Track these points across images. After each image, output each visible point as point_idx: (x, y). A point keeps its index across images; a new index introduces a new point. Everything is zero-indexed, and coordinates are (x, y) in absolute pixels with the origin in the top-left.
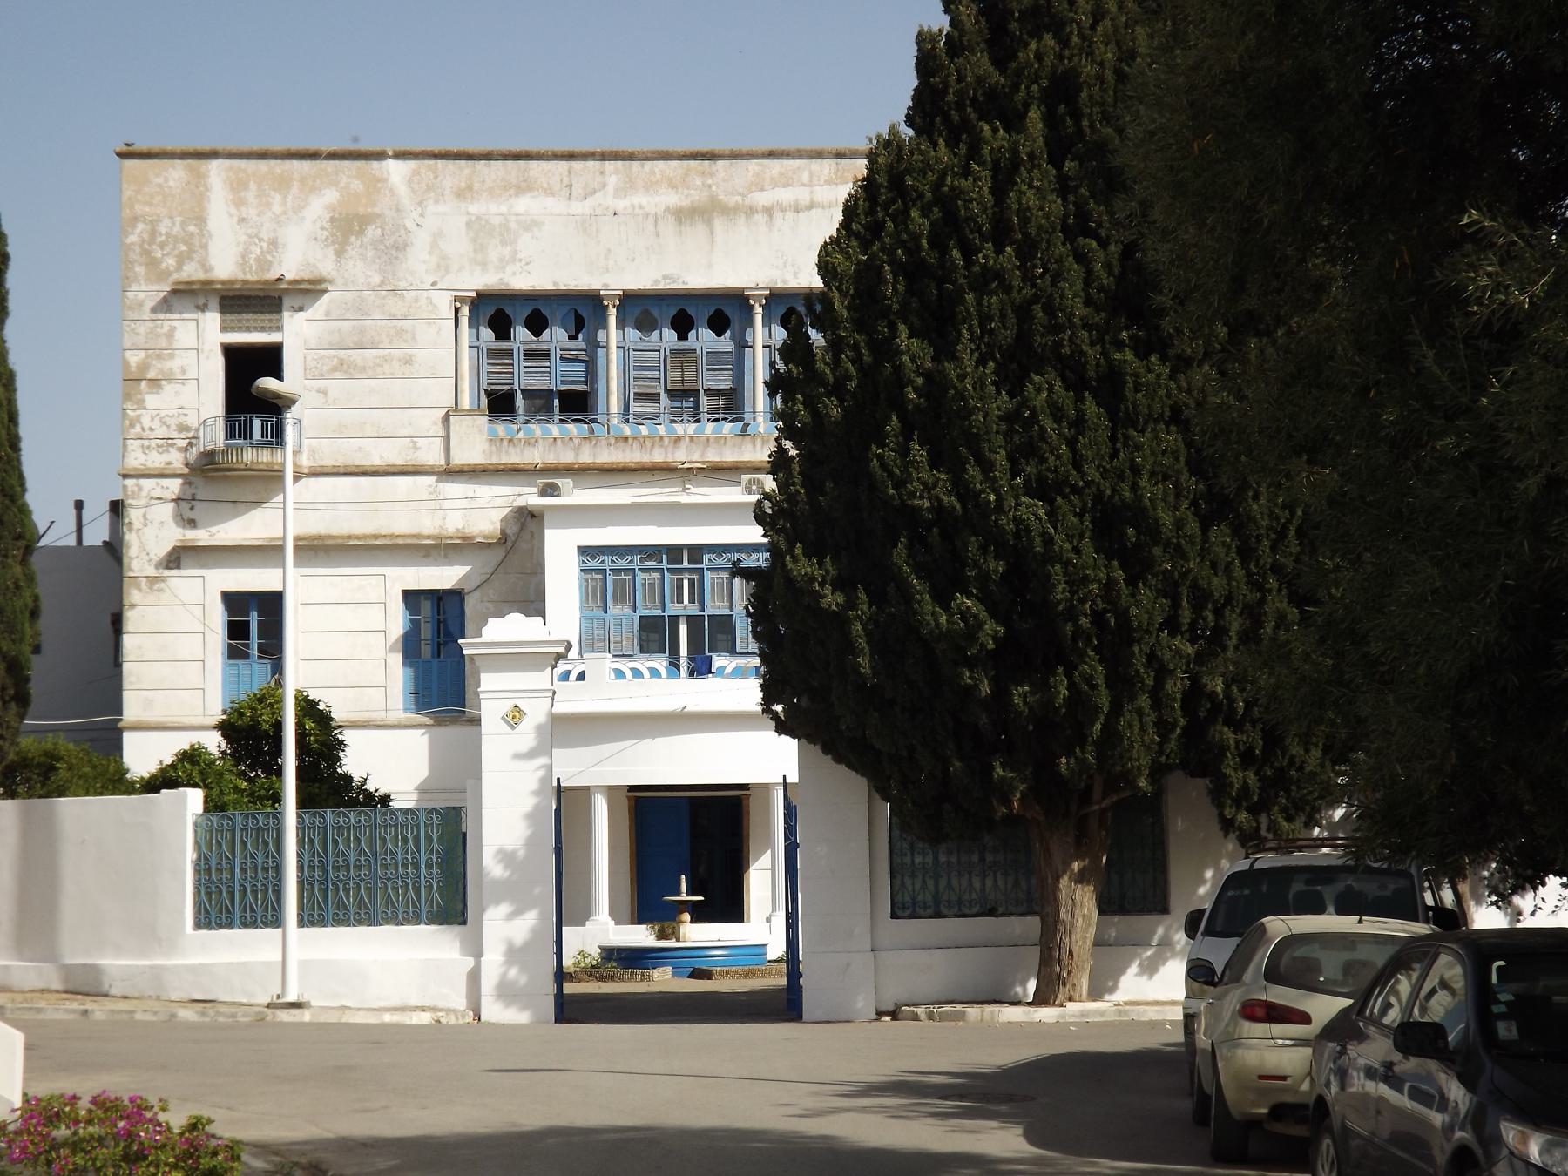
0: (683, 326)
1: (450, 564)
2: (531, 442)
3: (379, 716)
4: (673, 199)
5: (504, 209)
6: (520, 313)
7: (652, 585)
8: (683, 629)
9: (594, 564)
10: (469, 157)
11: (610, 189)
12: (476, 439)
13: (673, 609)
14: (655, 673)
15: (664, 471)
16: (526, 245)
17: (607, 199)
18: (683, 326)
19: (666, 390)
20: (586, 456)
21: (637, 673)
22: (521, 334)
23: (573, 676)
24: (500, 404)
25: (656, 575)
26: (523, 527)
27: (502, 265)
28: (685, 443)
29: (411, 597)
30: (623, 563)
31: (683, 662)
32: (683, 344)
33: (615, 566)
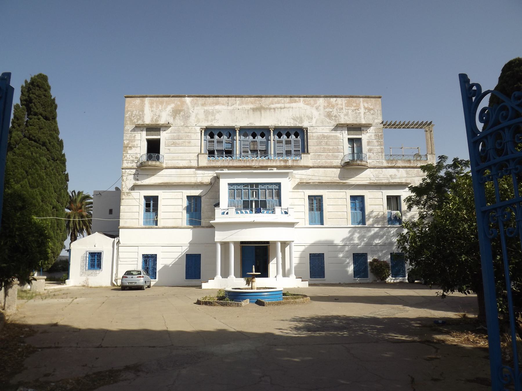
0: (254, 135)
2: (218, 161)
3: (180, 225)
4: (252, 106)
5: (213, 108)
6: (216, 133)
8: (254, 204)
9: (232, 188)
10: (205, 97)
11: (237, 104)
12: (204, 161)
13: (251, 199)
14: (246, 213)
15: (250, 167)
16: (218, 116)
17: (237, 106)
18: (254, 135)
19: (251, 150)
20: (231, 164)
21: (242, 213)
22: (216, 137)
23: (225, 213)
24: (211, 153)
27: (212, 121)
28: (254, 162)
29: (188, 197)
30: (239, 188)
31: (254, 210)
32: (254, 140)
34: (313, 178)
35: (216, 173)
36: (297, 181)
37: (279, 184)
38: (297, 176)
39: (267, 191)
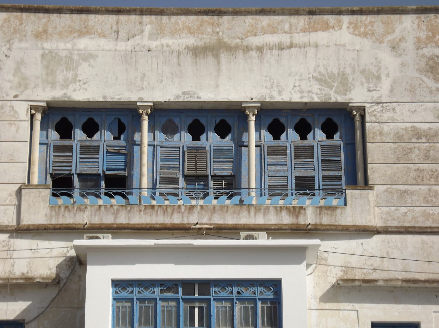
0: (196, 131)
1: (16, 300)
2: (82, 209)
4: (191, 41)
5: (69, 46)
6: (78, 121)
7: (170, 312)
9: (124, 294)
10: (47, 11)
11: (146, 33)
12: (40, 208)
15: (183, 230)
16: (85, 70)
17: (144, 41)
18: (196, 131)
20: (123, 219)
22: (79, 135)
24: (61, 184)
25: (173, 304)
26: (73, 272)
27: (66, 84)
28: (196, 211)
30: (147, 294)
32: (197, 144)
33: (140, 296)
34: (386, 264)
35: (76, 248)
36: (334, 275)
37: (275, 285)
38: (332, 259)
39: (237, 308)
